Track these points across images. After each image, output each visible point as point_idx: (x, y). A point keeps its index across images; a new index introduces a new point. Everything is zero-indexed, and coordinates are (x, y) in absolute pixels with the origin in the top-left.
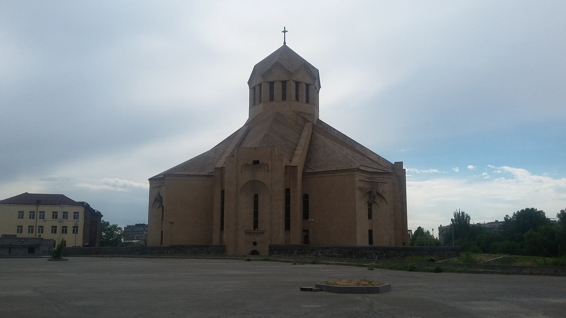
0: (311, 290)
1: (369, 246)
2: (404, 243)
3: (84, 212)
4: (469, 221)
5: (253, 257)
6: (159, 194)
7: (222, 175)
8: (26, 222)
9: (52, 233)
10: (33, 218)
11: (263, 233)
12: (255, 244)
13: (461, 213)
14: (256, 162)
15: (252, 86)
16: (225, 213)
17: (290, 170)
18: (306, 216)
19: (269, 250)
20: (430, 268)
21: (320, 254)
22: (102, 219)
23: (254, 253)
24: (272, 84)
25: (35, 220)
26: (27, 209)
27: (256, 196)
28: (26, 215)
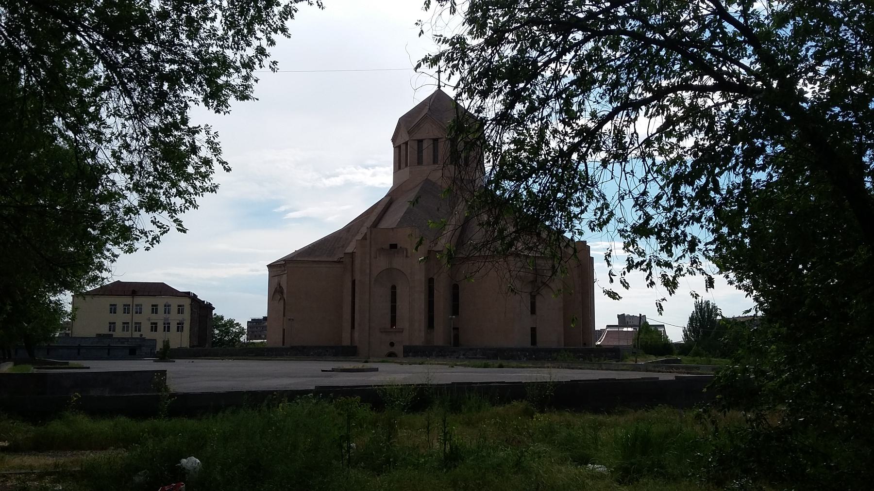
0: (326, 371)
1: (532, 347)
2: (585, 344)
3: (191, 304)
6: (280, 284)
7: (353, 262)
8: (120, 318)
9: (152, 331)
10: (128, 313)
11: (401, 331)
12: (392, 344)
13: (703, 302)
14: (394, 246)
15: (398, 143)
18: (455, 310)
19: (404, 352)
21: (461, 357)
22: (214, 312)
23: (391, 355)
24: (420, 142)
25: (129, 315)
26: (120, 301)
27: (394, 288)
28: (120, 309)
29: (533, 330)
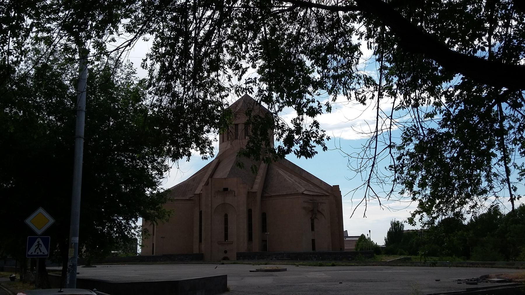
0: (254, 271)
1: (313, 251)
2: (341, 249)
4: (403, 229)
5: (225, 262)
11: (232, 243)
12: (226, 252)
13: (396, 222)
14: (226, 189)
16: (203, 228)
17: (250, 195)
18: (264, 228)
20: (329, 264)
21: (274, 259)
23: (225, 259)
27: (226, 216)
29: (313, 241)
